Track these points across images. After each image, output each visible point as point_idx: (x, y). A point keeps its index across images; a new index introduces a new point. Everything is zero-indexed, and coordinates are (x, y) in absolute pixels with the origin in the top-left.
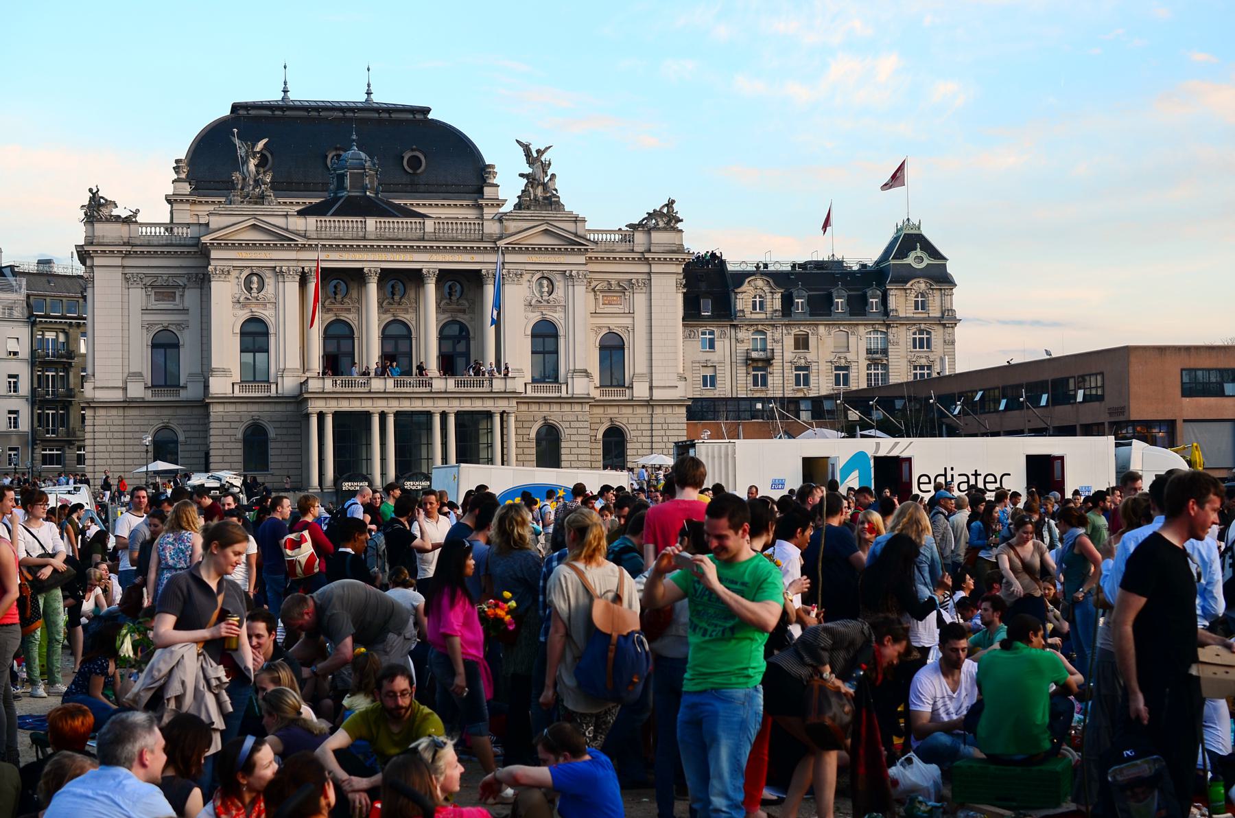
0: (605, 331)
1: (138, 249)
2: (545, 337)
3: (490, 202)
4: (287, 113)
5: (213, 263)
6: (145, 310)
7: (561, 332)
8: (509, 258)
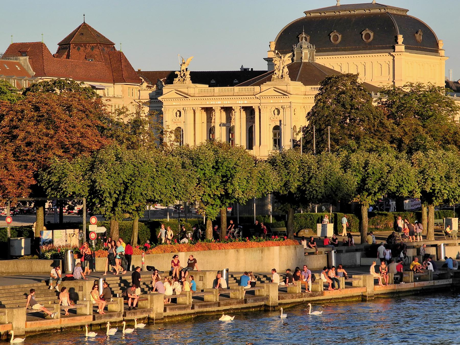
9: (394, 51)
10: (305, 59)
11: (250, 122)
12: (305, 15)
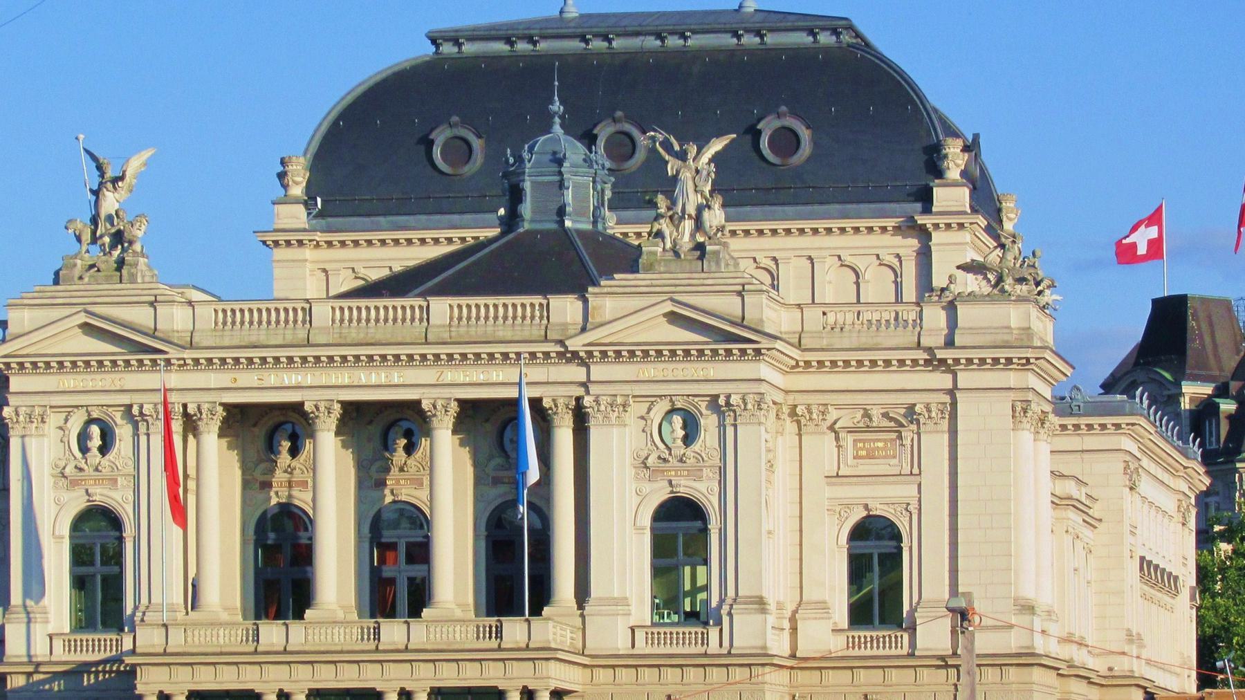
0: (858, 514)
2: (681, 529)
3: (942, 221)
4: (543, 46)
5: (12, 400)
8: (598, 372)
9: (927, 210)
10: (580, 213)
11: (496, 481)
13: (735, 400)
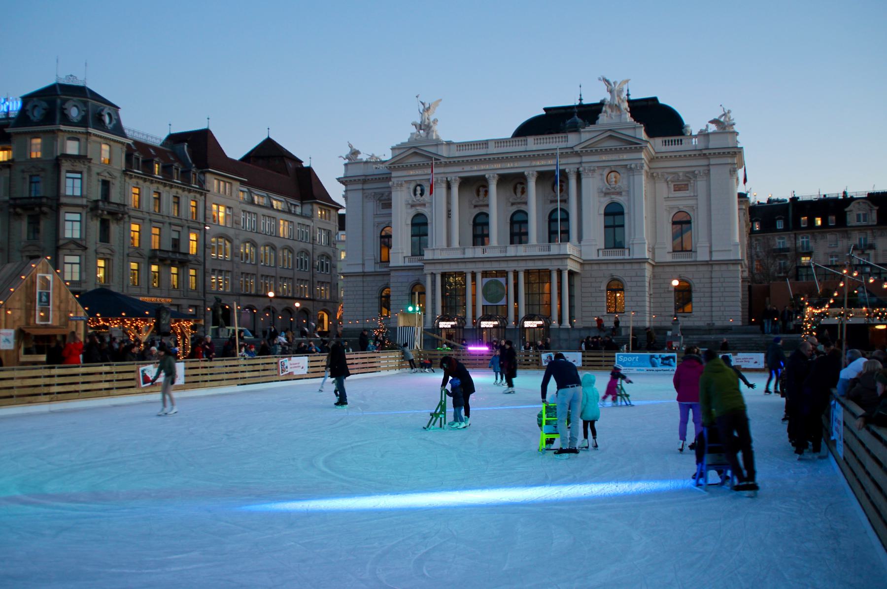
1: (370, 178)
2: (614, 215)
6: (376, 215)
7: (626, 211)
12: (544, 113)
13: (633, 166)
